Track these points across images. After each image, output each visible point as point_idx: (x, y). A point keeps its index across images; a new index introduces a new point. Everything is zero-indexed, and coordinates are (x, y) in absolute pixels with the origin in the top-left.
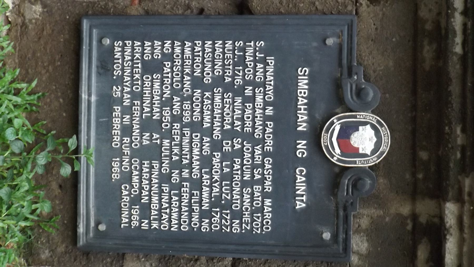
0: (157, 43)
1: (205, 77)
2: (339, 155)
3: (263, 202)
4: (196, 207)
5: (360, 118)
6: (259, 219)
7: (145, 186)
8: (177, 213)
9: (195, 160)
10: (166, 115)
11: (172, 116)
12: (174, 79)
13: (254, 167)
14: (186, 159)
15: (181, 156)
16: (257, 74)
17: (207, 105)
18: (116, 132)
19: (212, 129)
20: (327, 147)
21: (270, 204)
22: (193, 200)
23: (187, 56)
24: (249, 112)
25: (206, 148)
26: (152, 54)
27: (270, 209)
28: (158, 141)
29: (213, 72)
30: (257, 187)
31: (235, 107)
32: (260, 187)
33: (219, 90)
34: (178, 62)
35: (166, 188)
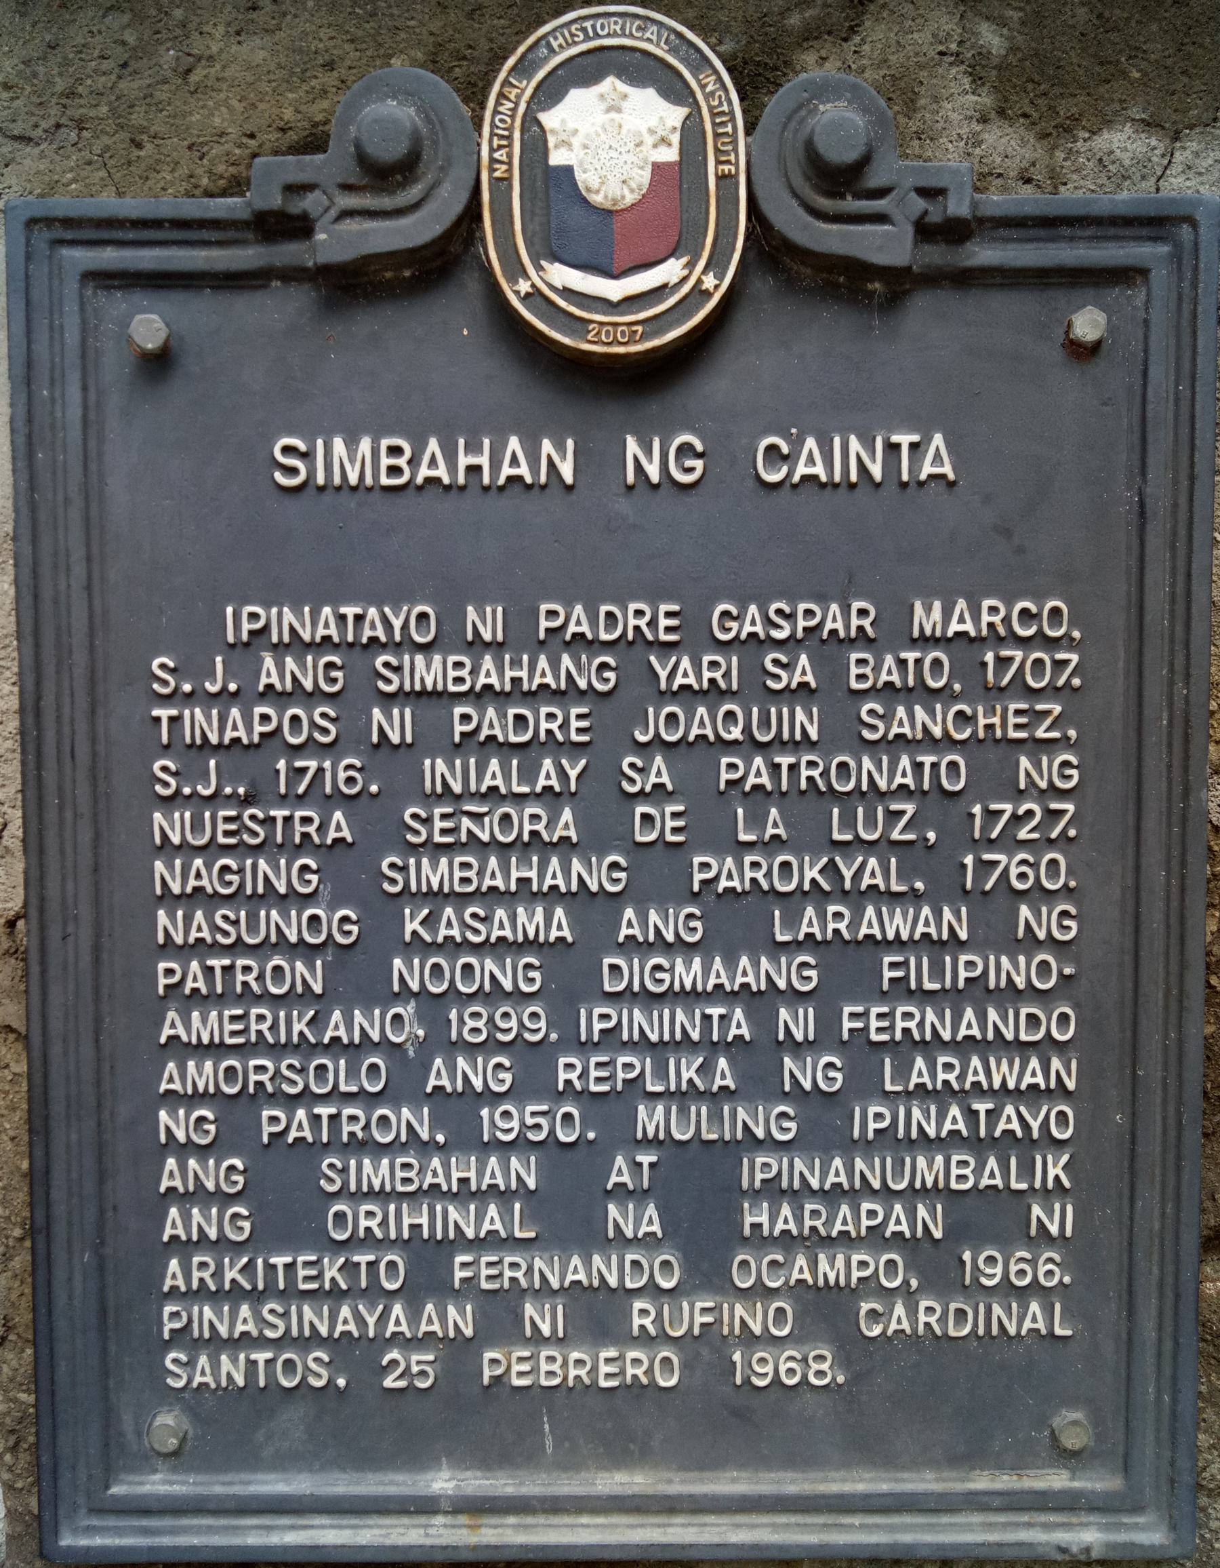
0: (171, 1175)
1: (330, 936)
2: (691, 265)
3: (926, 641)
4: (963, 967)
5: (510, 164)
7: (865, 1223)
8: (992, 1061)
9: (732, 979)
10: (515, 1124)
12: (343, 1088)
15: (711, 1048)
16: (308, 685)
17: (464, 925)
18: (604, 1369)
19: (580, 899)
20: (656, 324)
22: (928, 986)
23: (229, 1027)
24: (493, 722)
27: (961, 604)
28: (646, 1159)
29: (310, 898)
30: (854, 671)
31: (473, 788)
33: (392, 866)
34: (259, 1070)
35: (872, 1117)
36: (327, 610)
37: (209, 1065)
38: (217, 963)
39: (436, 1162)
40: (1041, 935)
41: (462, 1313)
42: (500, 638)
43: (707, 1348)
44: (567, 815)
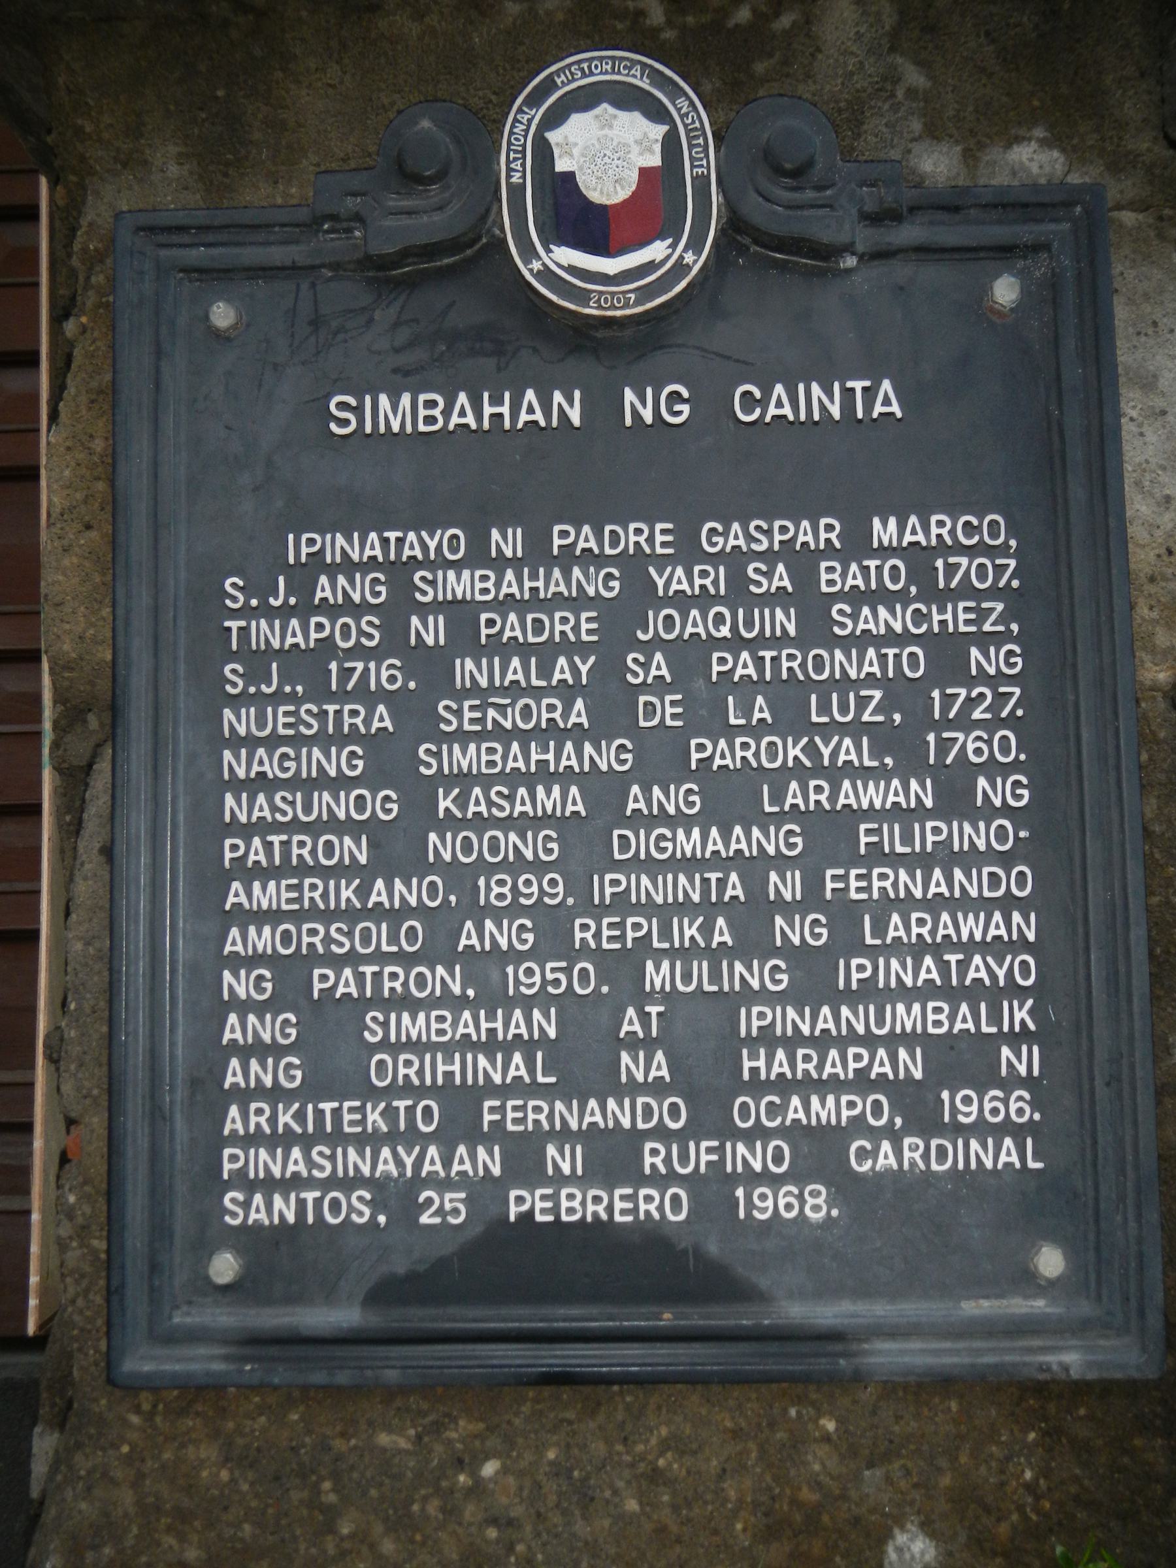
0: (232, 1030)
2: (674, 246)
3: (885, 552)
4: (930, 834)
6: (958, 565)
7: (852, 1065)
8: (960, 916)
9: (727, 846)
10: (537, 979)
11: (537, 954)
12: (385, 948)
13: (739, 592)
14: (722, 883)
15: (708, 909)
17: (490, 804)
18: (619, 1205)
19: (590, 780)
20: (646, 293)
21: (892, 522)
22: (899, 849)
23: (285, 895)
24: (512, 627)
25: (674, 799)
26: (277, 1050)
29: (354, 782)
30: (824, 577)
31: (497, 684)
32: (824, 565)
34: (312, 936)
35: (857, 970)
36: (373, 535)
37: (267, 930)
38: (276, 839)
39: (467, 1015)
40: (998, 802)
41: (491, 1154)
42: (519, 554)
43: (714, 1189)
44: (579, 704)
